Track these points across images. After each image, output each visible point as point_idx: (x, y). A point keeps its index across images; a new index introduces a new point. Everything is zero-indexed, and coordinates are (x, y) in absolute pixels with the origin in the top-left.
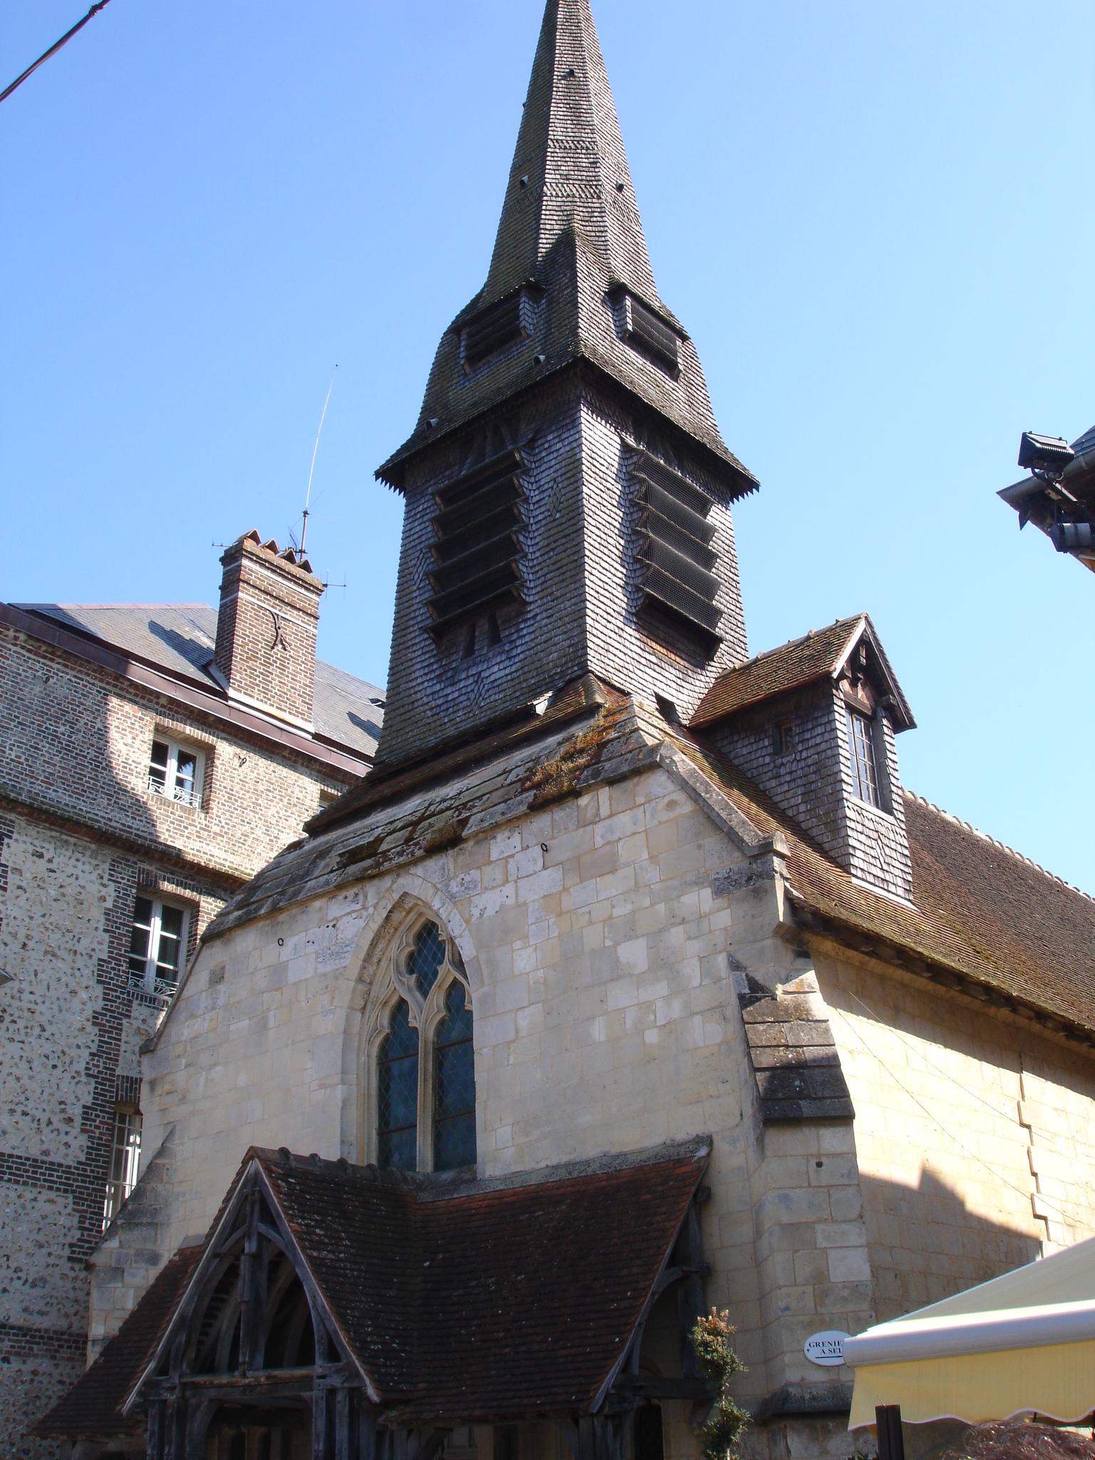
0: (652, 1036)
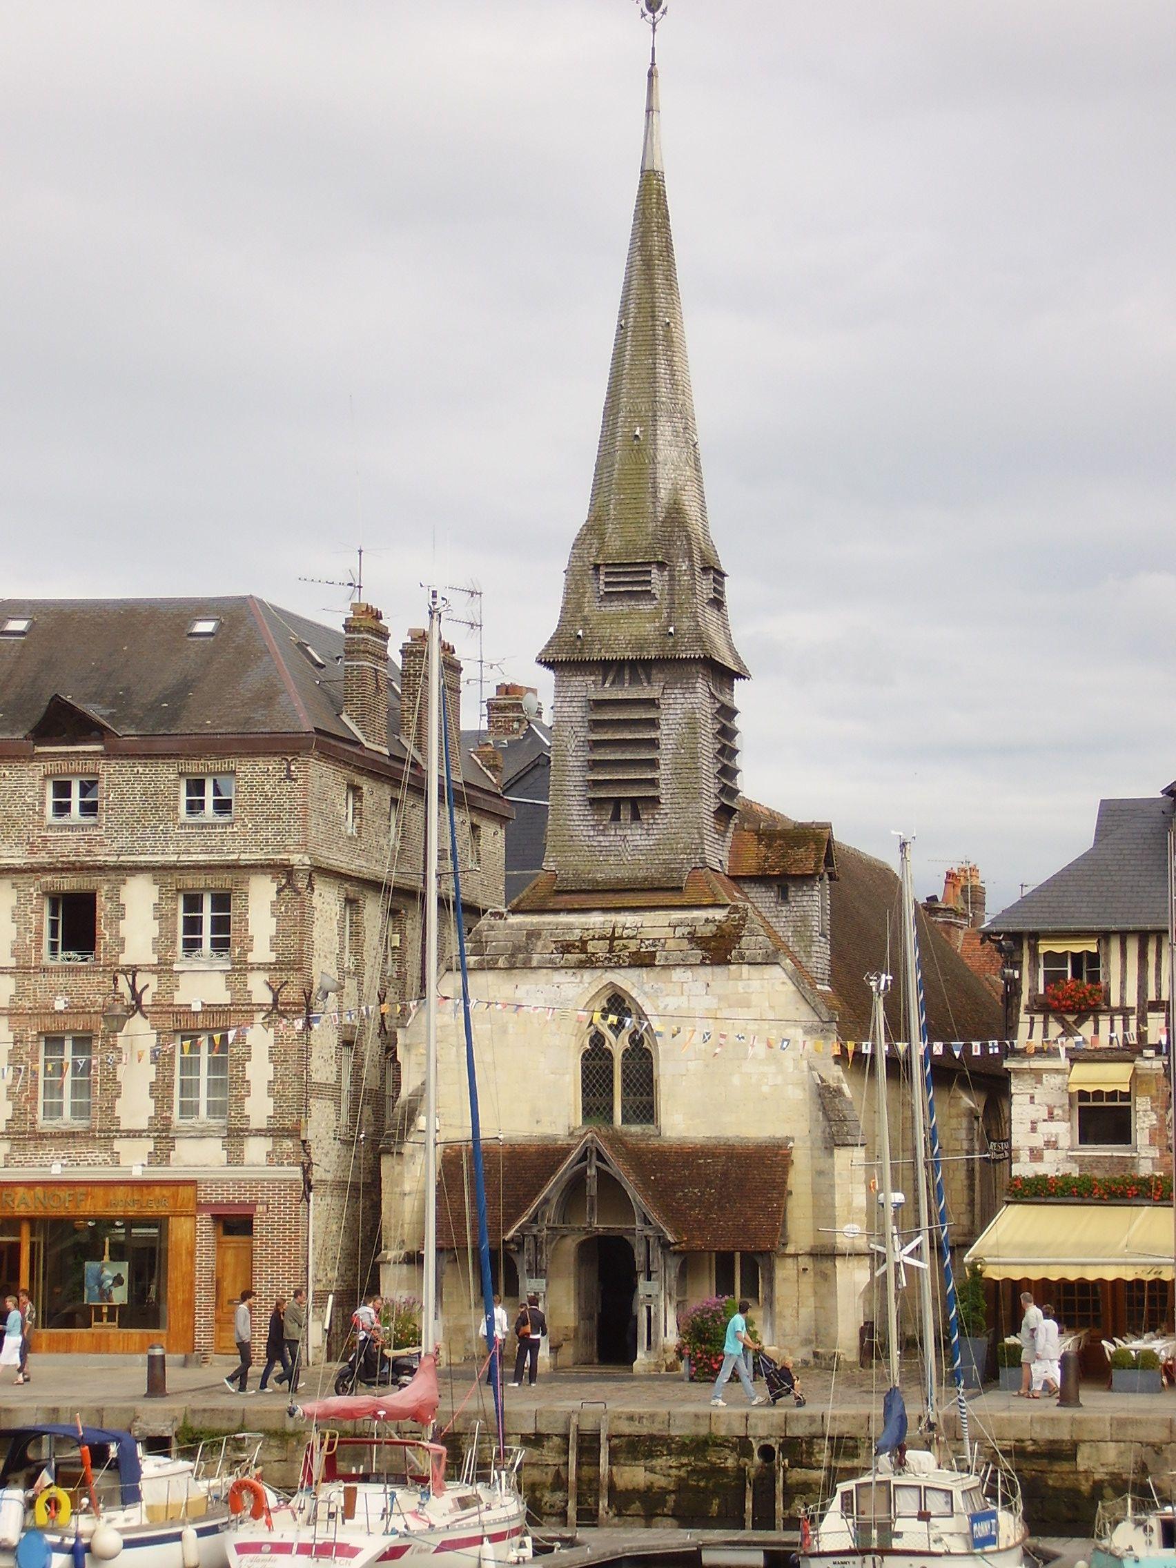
0: (765, 1089)
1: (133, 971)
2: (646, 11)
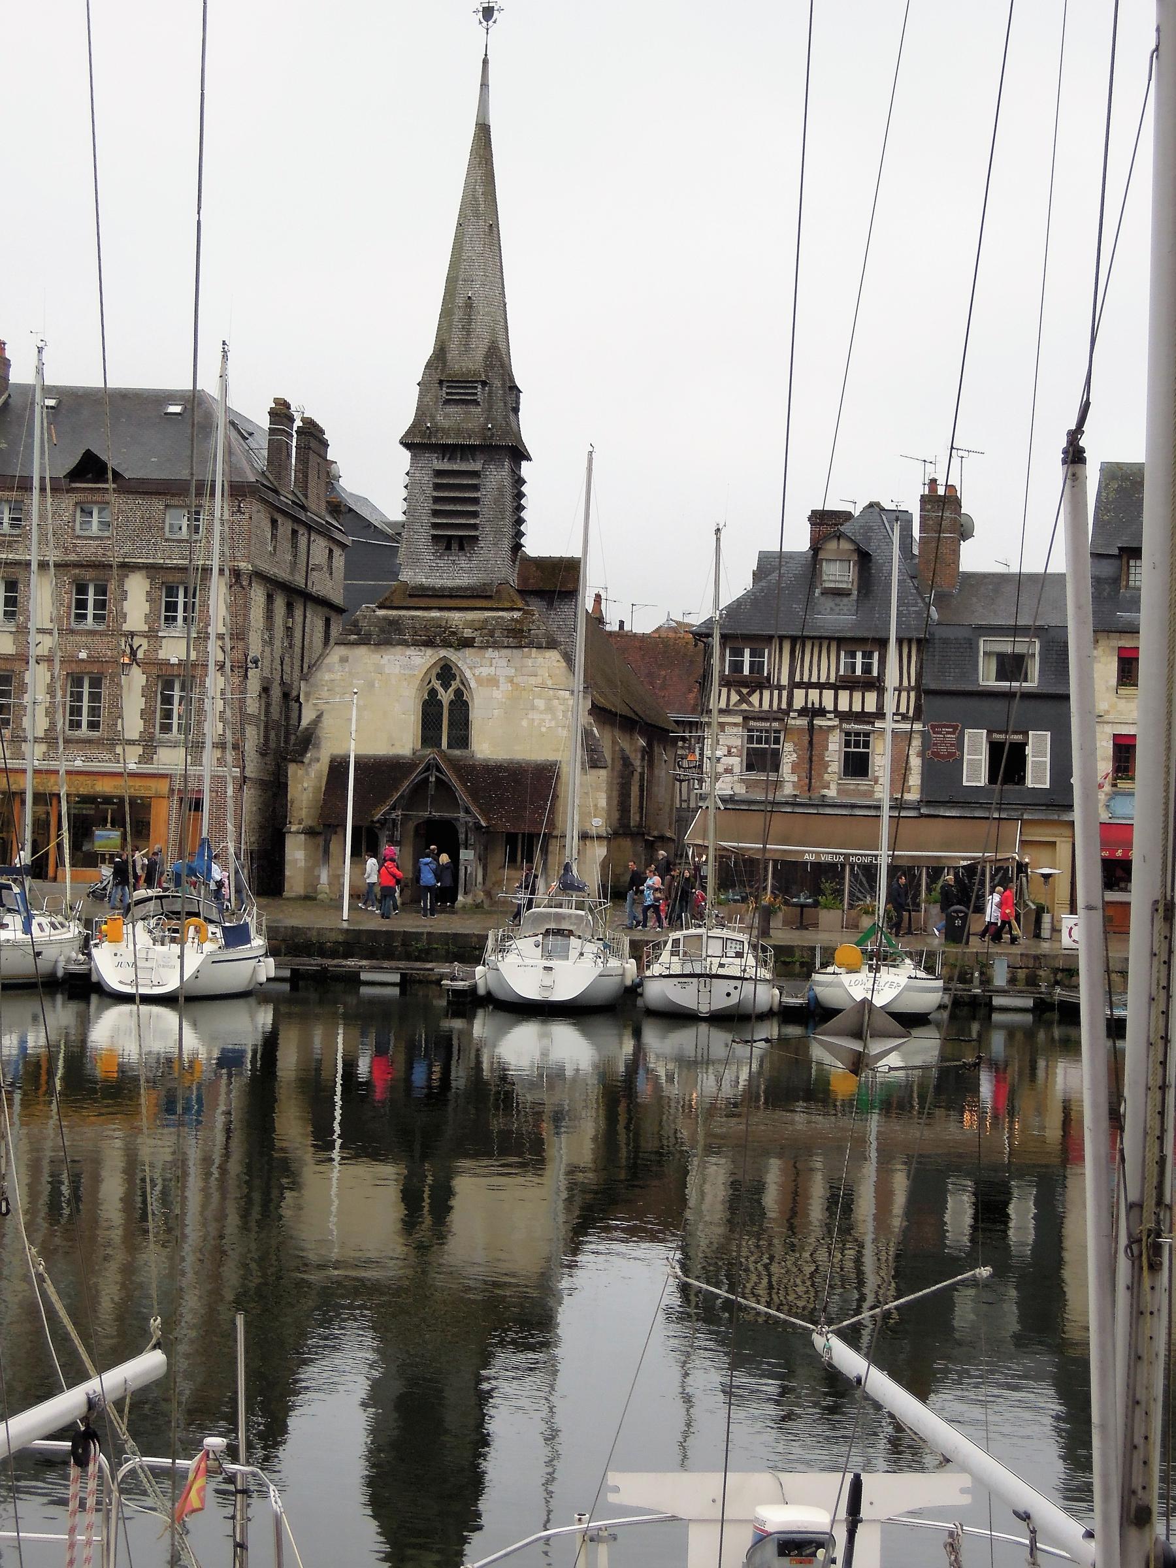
0: (544, 729)
1: (132, 634)
2: (482, 20)
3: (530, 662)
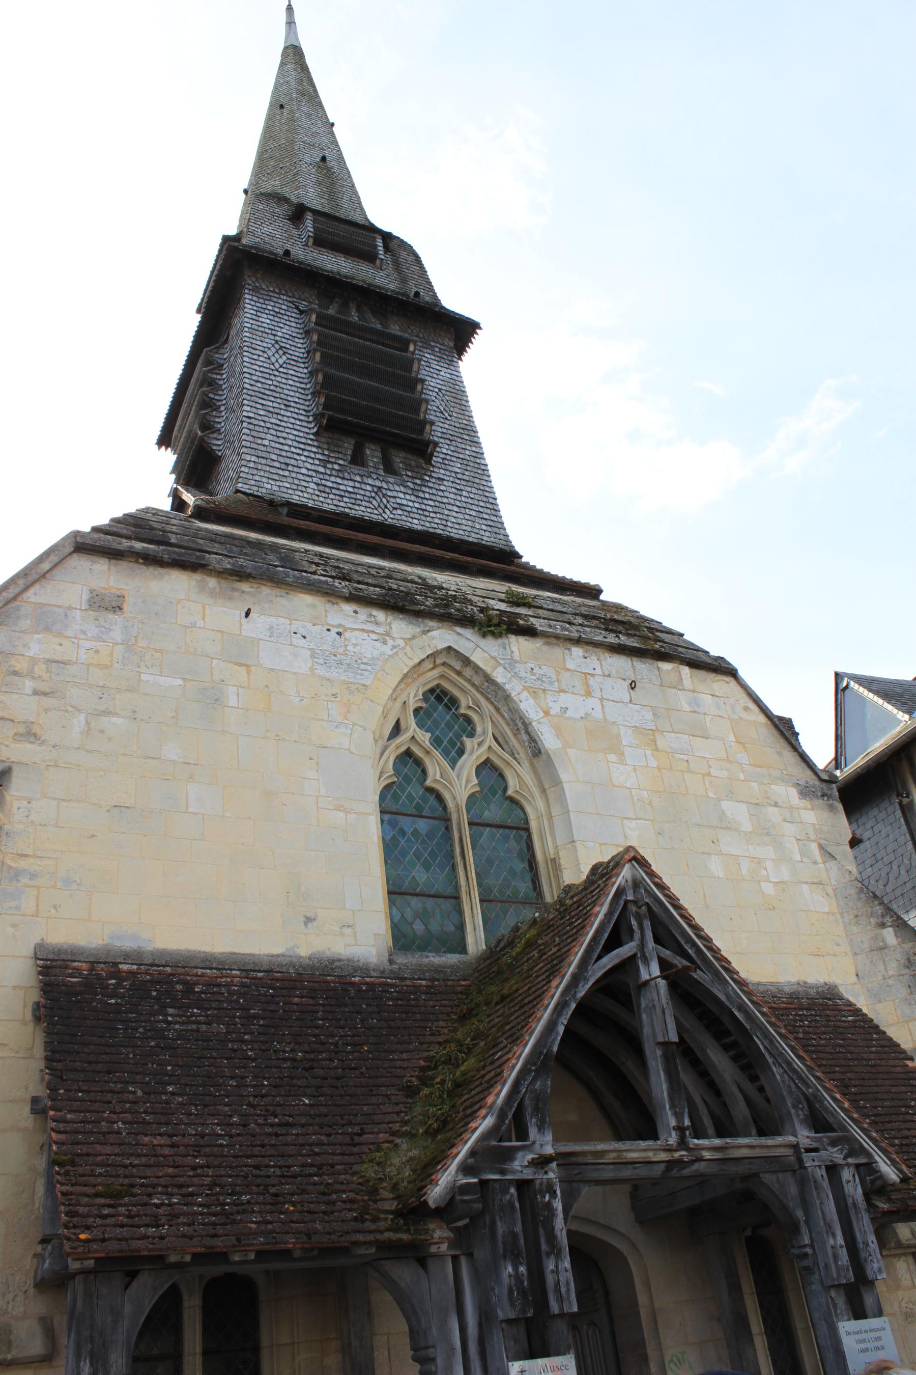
3: (682, 700)
